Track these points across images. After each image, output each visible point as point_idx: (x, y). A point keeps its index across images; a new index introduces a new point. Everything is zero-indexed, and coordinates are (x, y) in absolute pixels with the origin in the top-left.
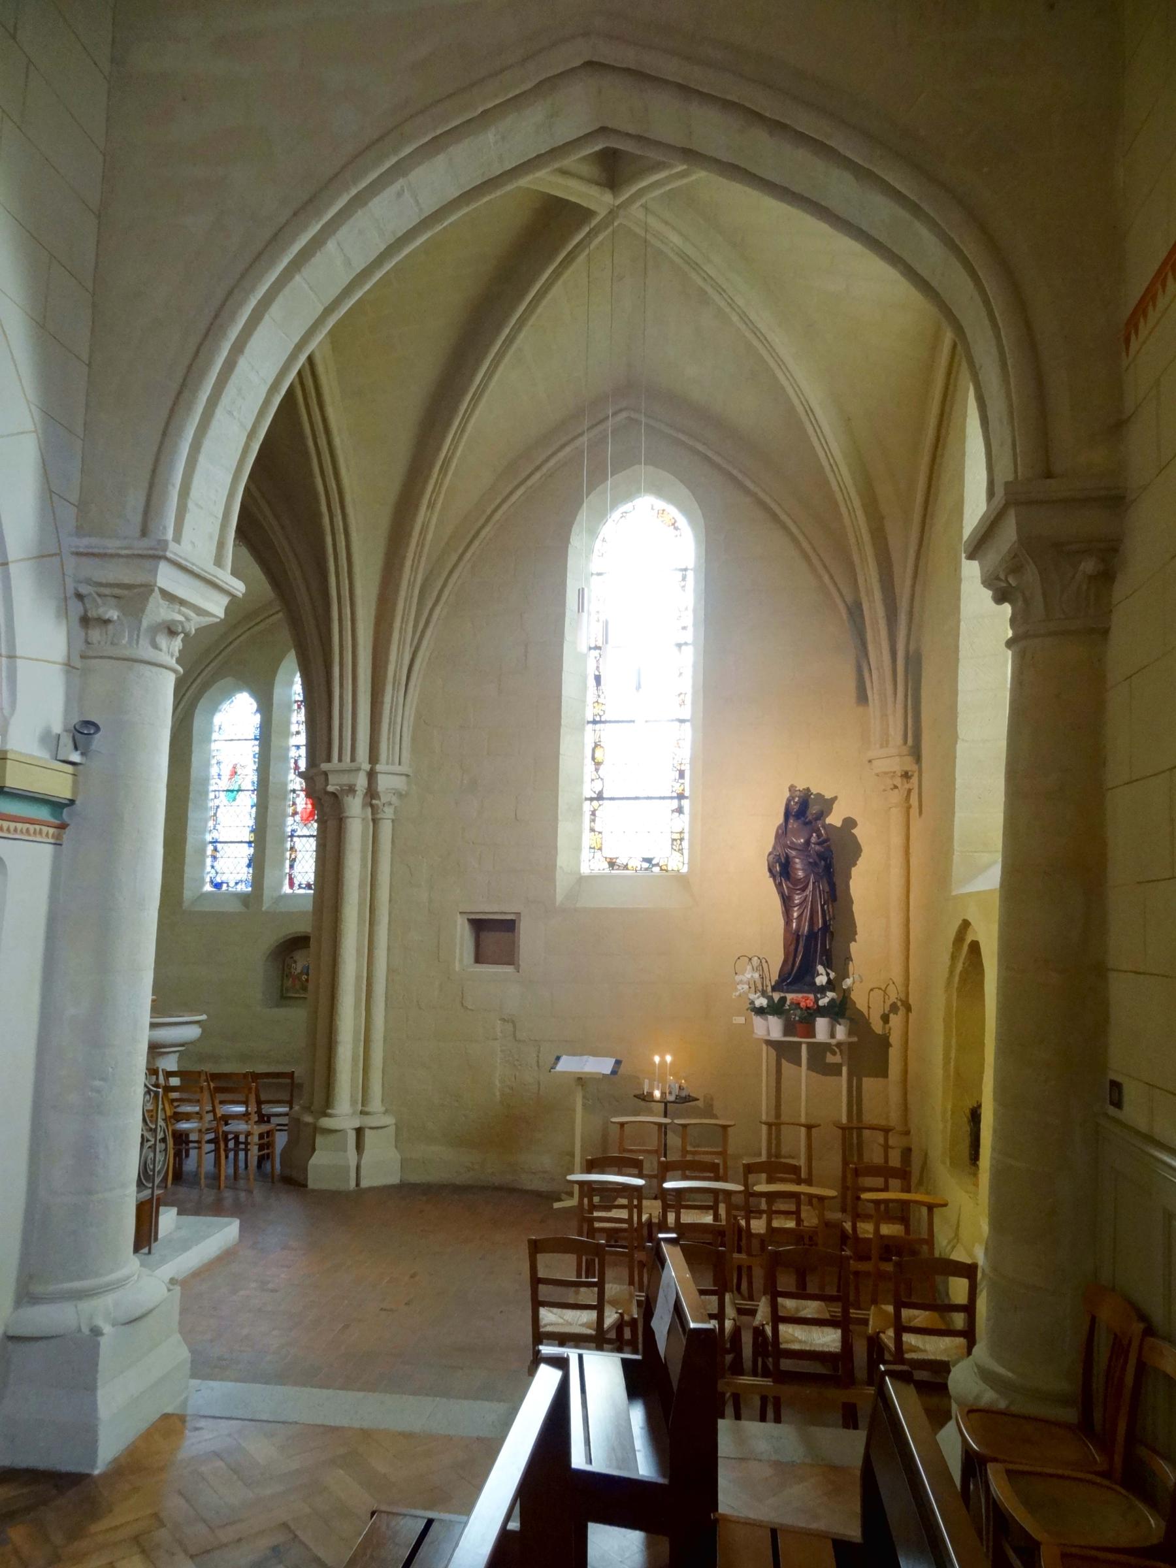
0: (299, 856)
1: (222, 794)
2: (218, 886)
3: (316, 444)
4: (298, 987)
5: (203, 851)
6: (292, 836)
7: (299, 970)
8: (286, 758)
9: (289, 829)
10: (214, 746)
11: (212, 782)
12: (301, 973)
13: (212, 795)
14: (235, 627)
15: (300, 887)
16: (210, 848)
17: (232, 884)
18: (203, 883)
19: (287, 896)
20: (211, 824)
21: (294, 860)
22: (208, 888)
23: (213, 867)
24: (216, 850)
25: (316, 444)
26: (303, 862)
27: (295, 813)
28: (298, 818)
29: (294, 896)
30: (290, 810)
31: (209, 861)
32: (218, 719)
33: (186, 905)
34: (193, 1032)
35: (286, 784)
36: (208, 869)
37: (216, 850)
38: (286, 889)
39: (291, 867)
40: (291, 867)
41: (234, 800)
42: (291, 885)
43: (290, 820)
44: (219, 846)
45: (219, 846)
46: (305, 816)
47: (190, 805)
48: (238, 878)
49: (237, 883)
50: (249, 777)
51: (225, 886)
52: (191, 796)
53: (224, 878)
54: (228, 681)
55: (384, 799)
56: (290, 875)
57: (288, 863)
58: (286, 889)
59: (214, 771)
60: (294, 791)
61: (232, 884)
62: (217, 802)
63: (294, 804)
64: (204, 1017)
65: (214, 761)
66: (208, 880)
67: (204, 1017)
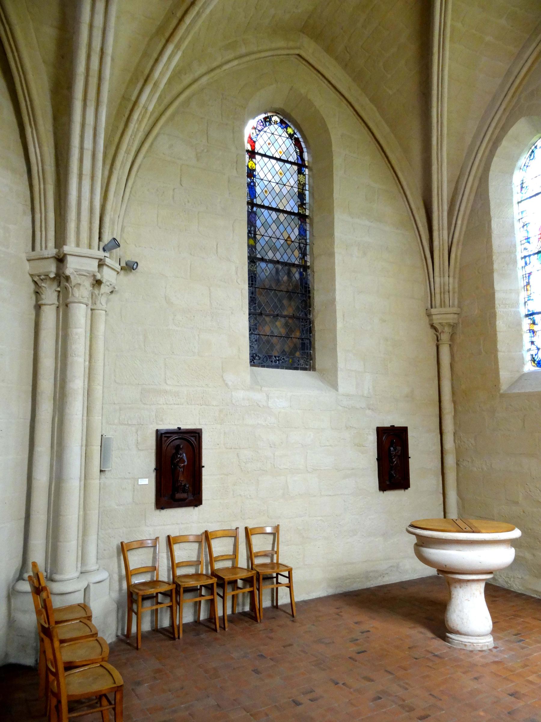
1: (534, 258)
10: (516, 209)
11: (519, 248)
13: (521, 263)
18: (523, 364)
20: (523, 295)
22: (529, 367)
23: (532, 343)
24: (534, 323)
31: (527, 337)
32: (517, 177)
33: (504, 388)
34: (501, 557)
36: (527, 344)
47: (496, 276)
52: (496, 266)
54: (521, 126)
59: (519, 235)
62: (528, 269)
64: (516, 533)
65: (518, 226)
66: (527, 357)
67: (516, 533)
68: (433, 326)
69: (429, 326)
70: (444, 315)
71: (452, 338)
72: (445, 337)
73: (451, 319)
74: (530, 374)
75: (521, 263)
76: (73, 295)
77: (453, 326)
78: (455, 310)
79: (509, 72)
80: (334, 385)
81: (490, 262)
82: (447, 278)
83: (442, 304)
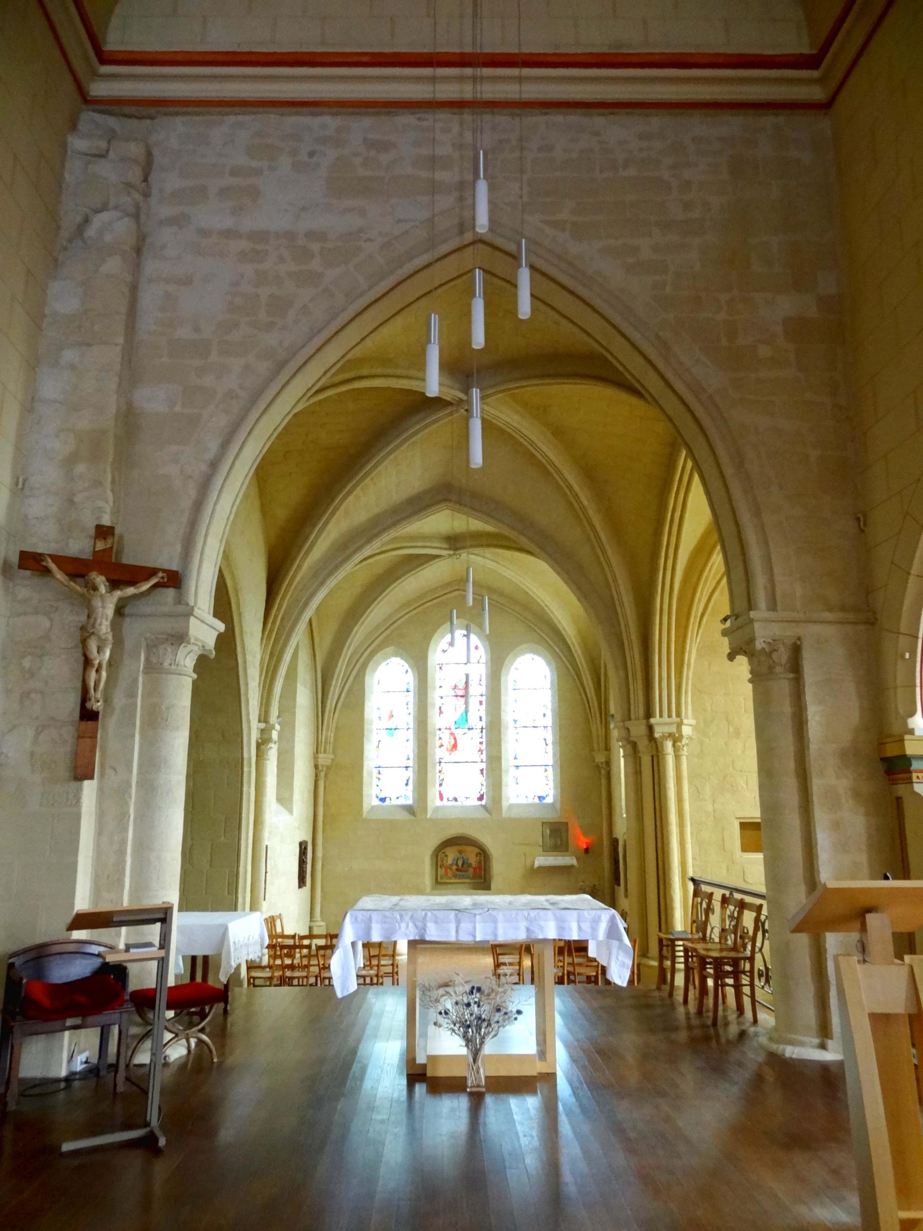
2: (383, 800)
3: (672, 516)
4: (450, 875)
5: (370, 774)
6: (440, 762)
7: (450, 861)
8: (433, 705)
12: (452, 865)
13: (375, 731)
14: (398, 610)
16: (375, 771)
19: (437, 809)
24: (379, 773)
25: (672, 516)
27: (442, 746)
29: (444, 807)
30: (438, 743)
31: (375, 781)
33: (364, 814)
39: (441, 785)
40: (441, 785)
42: (441, 798)
46: (450, 748)
50: (406, 717)
51: (388, 800)
55: (684, 741)
57: (438, 783)
58: (438, 803)
61: (394, 798)
66: (374, 796)
68: (316, 767)
69: (313, 765)
70: (324, 759)
71: (326, 776)
72: (322, 774)
73: (329, 762)
74: (378, 806)
77: (328, 768)
78: (332, 756)
79: (390, 616)
80: (290, 811)
83: (325, 752)
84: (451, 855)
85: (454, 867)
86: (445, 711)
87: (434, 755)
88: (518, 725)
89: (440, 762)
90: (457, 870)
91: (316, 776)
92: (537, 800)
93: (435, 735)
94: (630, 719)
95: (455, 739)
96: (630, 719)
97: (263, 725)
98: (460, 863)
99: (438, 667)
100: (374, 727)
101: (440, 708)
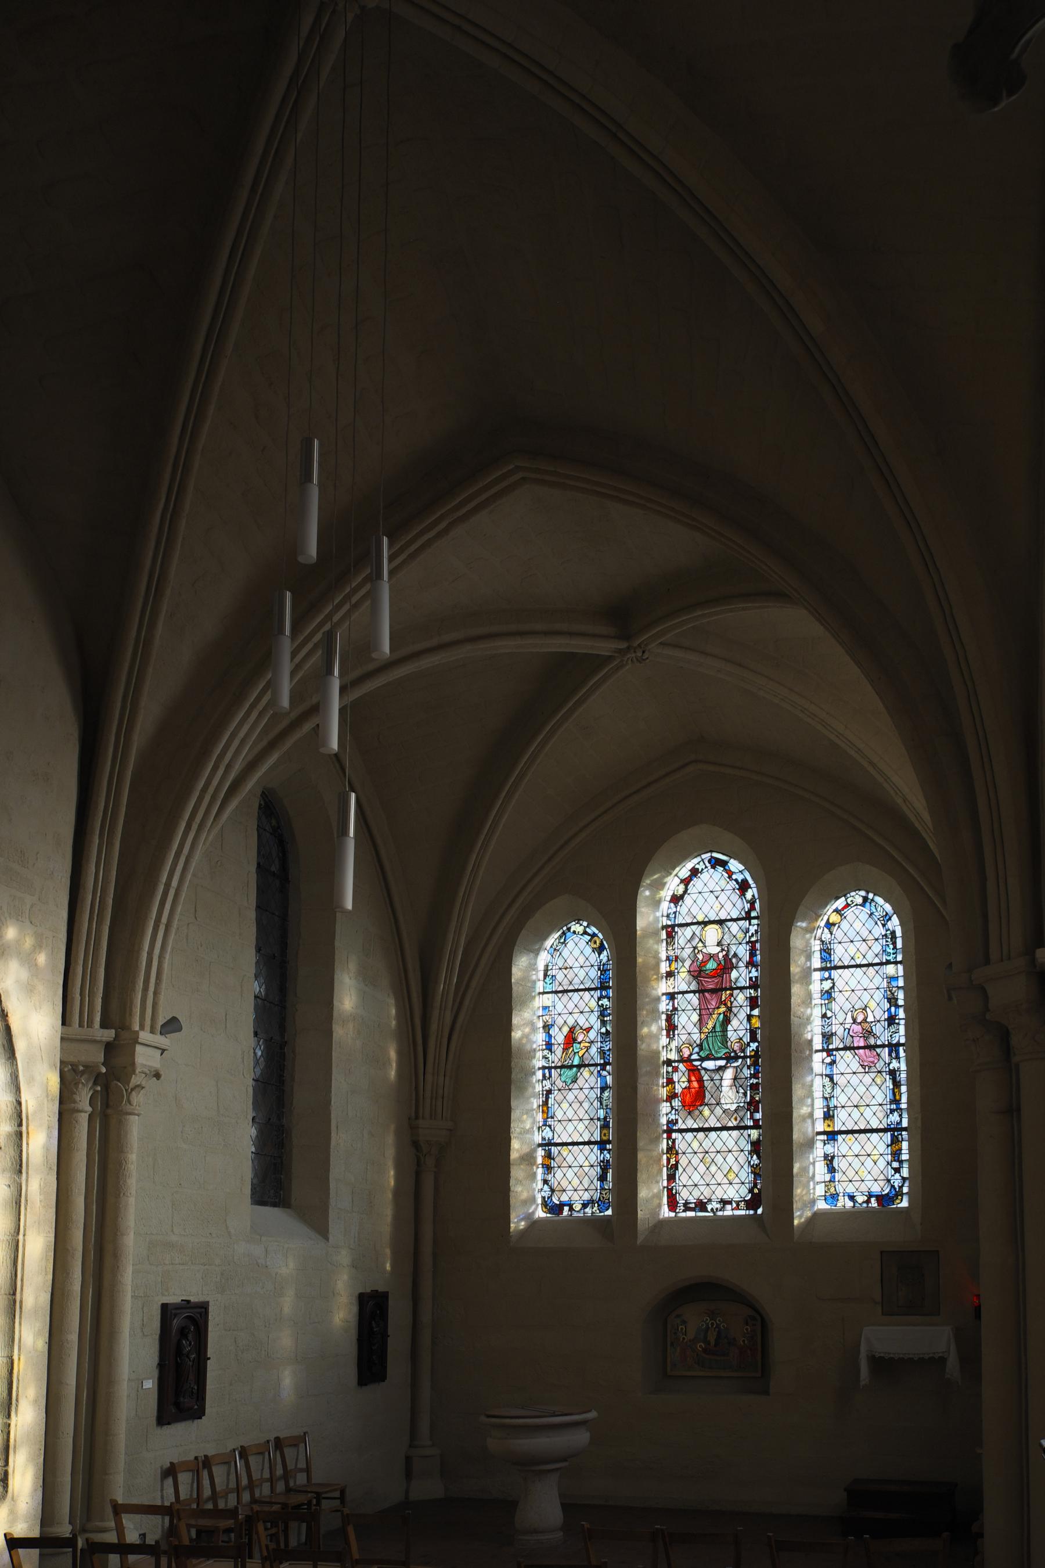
0: (683, 1161)
5: (529, 1159)
6: (669, 1132)
9: (664, 1120)
15: (687, 1208)
16: (540, 1153)
17: (577, 1207)
21: (676, 1167)
23: (545, 1182)
26: (690, 1170)
28: (676, 1103)
30: (664, 1092)
35: (657, 1053)
37: (549, 1156)
38: (666, 1213)
39: (671, 1178)
40: (671, 1178)
41: (575, 1080)
42: (673, 1205)
43: (665, 1108)
44: (554, 1150)
45: (554, 1150)
47: (513, 1088)
48: (586, 1196)
49: (585, 1206)
53: (564, 1198)
56: (670, 1191)
58: (666, 1213)
60: (669, 1062)
61: (577, 1207)
63: (670, 1081)
68: (416, 1145)
75: (539, 1074)
76: (129, 1102)
80: (323, 1231)
81: (509, 1070)
82: (441, 1078)
84: (693, 1321)
85: (700, 1346)
86: (675, 1023)
87: (655, 1115)
88: (836, 1043)
89: (669, 1132)
90: (705, 1351)
91: (418, 1164)
92: (874, 1203)
93: (658, 1074)
94: (987, 961)
95: (700, 1081)
96: (987, 961)
97: (109, 1034)
98: (712, 1337)
99: (664, 935)
100: (539, 1063)
101: (669, 1019)
